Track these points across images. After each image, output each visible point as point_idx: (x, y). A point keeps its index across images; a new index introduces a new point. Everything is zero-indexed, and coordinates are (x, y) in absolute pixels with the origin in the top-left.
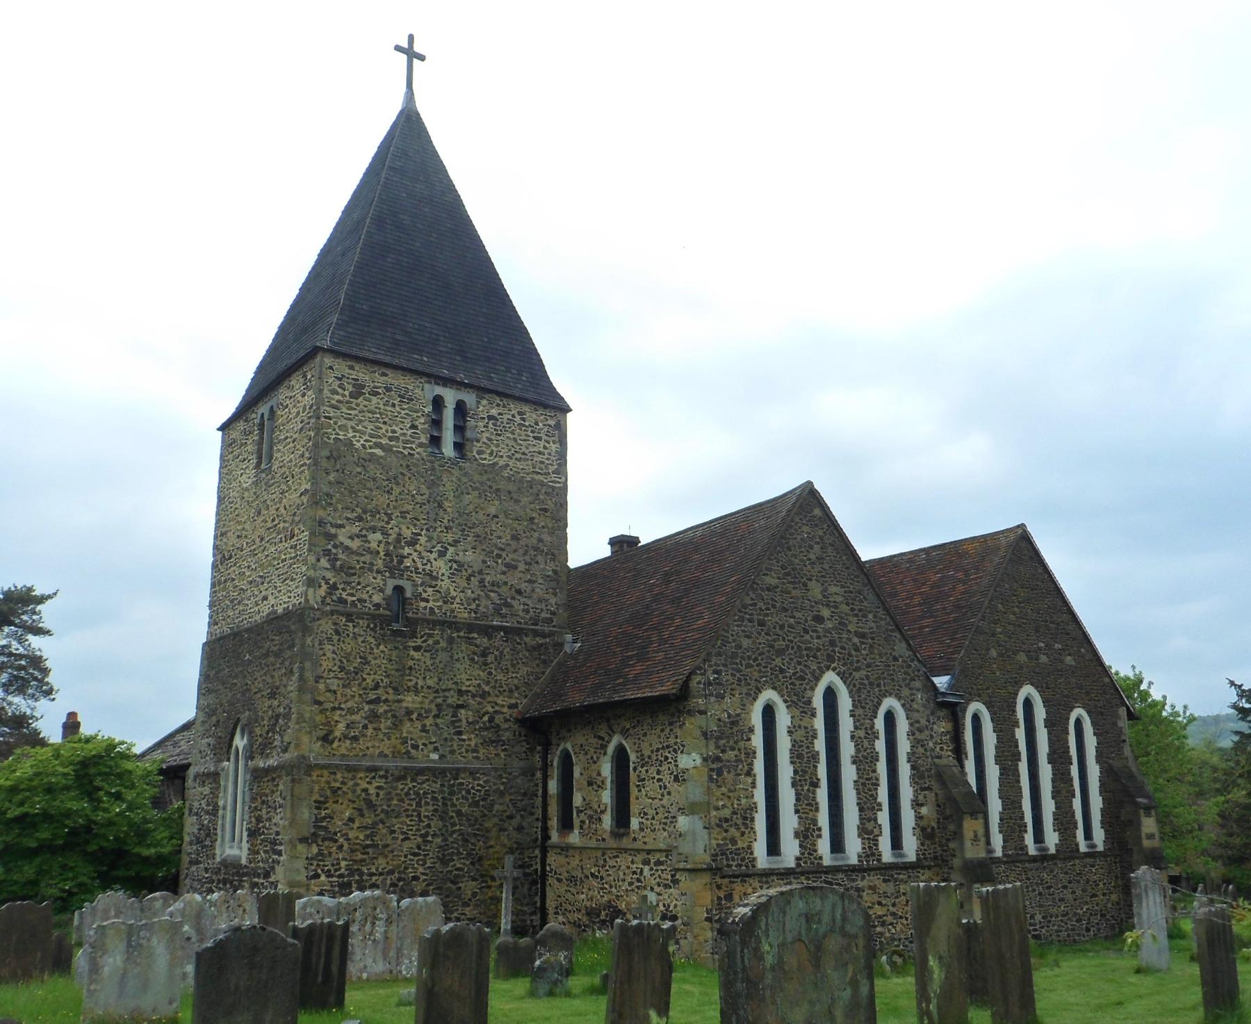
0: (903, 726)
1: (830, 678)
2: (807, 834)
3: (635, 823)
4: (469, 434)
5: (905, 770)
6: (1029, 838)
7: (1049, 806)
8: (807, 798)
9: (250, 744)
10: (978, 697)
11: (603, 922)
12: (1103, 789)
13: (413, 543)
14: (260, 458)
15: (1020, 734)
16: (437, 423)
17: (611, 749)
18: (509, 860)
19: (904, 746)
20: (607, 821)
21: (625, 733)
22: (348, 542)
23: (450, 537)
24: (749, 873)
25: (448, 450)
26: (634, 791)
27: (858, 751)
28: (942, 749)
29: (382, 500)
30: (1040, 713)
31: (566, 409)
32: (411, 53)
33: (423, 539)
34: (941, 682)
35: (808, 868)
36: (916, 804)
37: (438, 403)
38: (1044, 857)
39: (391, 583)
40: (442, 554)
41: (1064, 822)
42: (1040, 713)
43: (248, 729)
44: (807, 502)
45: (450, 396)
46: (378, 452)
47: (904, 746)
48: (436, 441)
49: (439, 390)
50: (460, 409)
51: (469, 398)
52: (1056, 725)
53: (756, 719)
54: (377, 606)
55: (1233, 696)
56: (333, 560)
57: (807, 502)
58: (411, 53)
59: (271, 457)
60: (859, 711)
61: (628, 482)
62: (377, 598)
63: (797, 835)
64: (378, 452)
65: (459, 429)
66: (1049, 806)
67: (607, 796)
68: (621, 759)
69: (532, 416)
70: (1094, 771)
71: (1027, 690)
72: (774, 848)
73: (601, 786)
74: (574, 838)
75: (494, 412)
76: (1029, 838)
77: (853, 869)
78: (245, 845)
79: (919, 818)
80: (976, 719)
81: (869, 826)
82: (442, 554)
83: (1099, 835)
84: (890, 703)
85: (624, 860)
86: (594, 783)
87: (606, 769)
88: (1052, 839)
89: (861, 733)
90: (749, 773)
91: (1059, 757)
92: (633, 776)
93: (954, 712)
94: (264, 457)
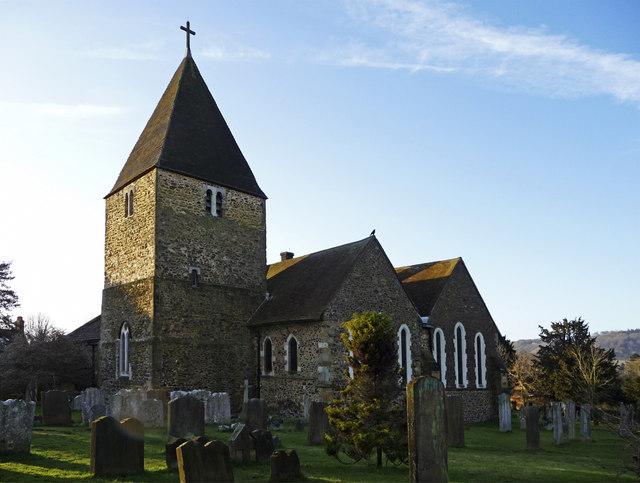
0: (408, 336)
3: (299, 369)
4: (223, 207)
6: (457, 382)
7: (465, 370)
9: (130, 332)
10: (440, 326)
11: (285, 407)
12: (487, 365)
13: (200, 252)
14: (126, 212)
15: (455, 341)
16: (209, 201)
17: (289, 339)
18: (246, 382)
20: (287, 368)
21: (294, 333)
22: (172, 250)
23: (216, 250)
25: (214, 213)
26: (298, 356)
29: (186, 233)
30: (464, 334)
31: (265, 198)
32: (188, 30)
33: (204, 251)
34: (425, 319)
36: (413, 366)
37: (209, 193)
38: (462, 389)
39: (191, 269)
40: (213, 258)
41: (471, 376)
42: (464, 334)
43: (128, 326)
44: (372, 243)
45: (214, 190)
46: (184, 212)
48: (209, 209)
49: (209, 187)
50: (219, 195)
51: (223, 191)
52: (470, 339)
54: (186, 277)
55: (540, 331)
56: (166, 258)
57: (372, 243)
58: (188, 30)
59: (132, 213)
61: (293, 231)
62: (185, 275)
64: (184, 212)
65: (219, 205)
66: (465, 370)
67: (287, 358)
68: (293, 344)
69: (251, 199)
70: (484, 358)
71: (459, 324)
73: (284, 354)
74: (272, 374)
75: (234, 198)
76: (457, 382)
78: (130, 373)
79: (414, 371)
80: (438, 334)
82: (213, 258)
83: (484, 382)
84: (404, 326)
85: (294, 383)
86: (281, 353)
87: (287, 348)
88: (466, 383)
91: (470, 351)
92: (298, 351)
93: (430, 332)
94: (129, 210)
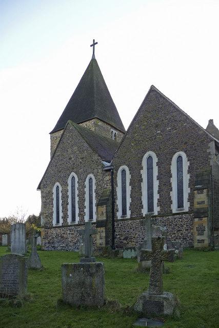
0: (94, 181)
1: (73, 174)
2: (65, 217)
5: (94, 195)
8: (65, 208)
19: (94, 187)
24: (52, 227)
27: (79, 192)
28: (107, 186)
35: (65, 226)
47: (94, 187)
53: (54, 191)
60: (81, 181)
63: (62, 218)
72: (58, 221)
77: (77, 225)
81: (82, 213)
89: (81, 187)
90: (52, 204)
93: (112, 172)
